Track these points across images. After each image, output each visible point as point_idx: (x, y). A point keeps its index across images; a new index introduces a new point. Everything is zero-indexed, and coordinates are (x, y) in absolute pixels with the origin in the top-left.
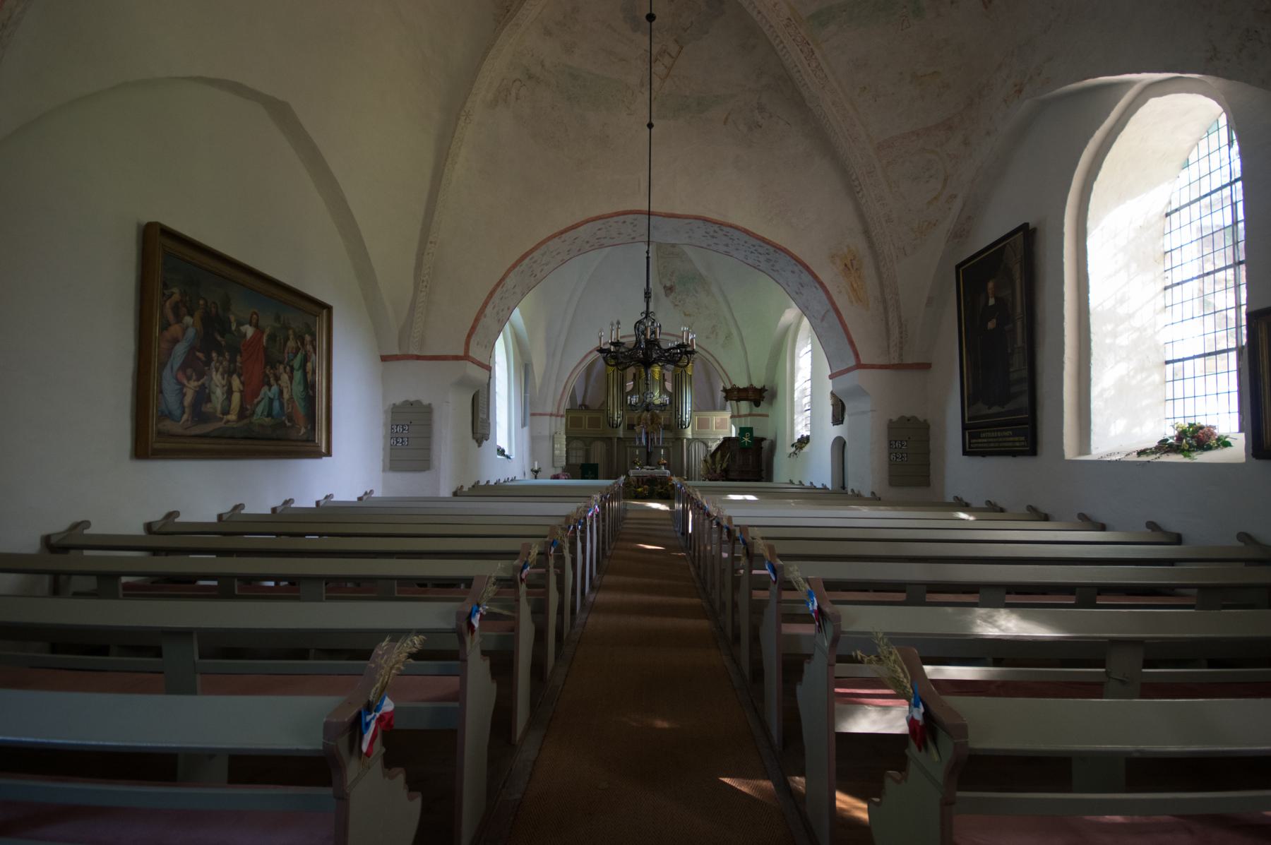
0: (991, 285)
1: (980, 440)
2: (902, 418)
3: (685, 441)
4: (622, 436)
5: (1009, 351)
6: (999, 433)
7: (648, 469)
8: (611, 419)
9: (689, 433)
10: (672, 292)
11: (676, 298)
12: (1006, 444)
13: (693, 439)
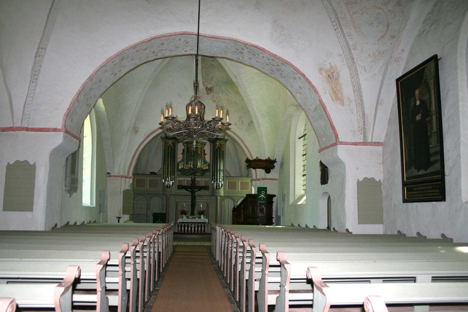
0: (417, 92)
1: (413, 193)
2: (365, 178)
5: (429, 134)
6: (424, 187)
9: (222, 192)
10: (211, 91)
11: (214, 96)
12: (428, 195)
13: (224, 196)
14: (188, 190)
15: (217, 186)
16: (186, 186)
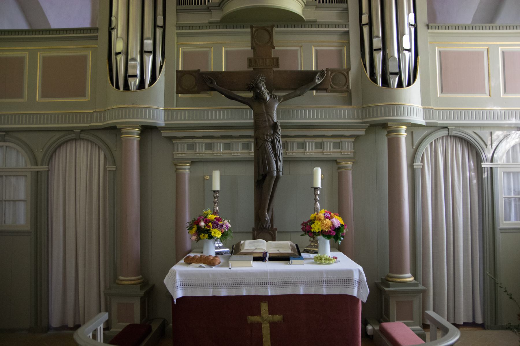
7: (260, 258)
8: (121, 59)
13: (428, 126)
16: (224, 71)
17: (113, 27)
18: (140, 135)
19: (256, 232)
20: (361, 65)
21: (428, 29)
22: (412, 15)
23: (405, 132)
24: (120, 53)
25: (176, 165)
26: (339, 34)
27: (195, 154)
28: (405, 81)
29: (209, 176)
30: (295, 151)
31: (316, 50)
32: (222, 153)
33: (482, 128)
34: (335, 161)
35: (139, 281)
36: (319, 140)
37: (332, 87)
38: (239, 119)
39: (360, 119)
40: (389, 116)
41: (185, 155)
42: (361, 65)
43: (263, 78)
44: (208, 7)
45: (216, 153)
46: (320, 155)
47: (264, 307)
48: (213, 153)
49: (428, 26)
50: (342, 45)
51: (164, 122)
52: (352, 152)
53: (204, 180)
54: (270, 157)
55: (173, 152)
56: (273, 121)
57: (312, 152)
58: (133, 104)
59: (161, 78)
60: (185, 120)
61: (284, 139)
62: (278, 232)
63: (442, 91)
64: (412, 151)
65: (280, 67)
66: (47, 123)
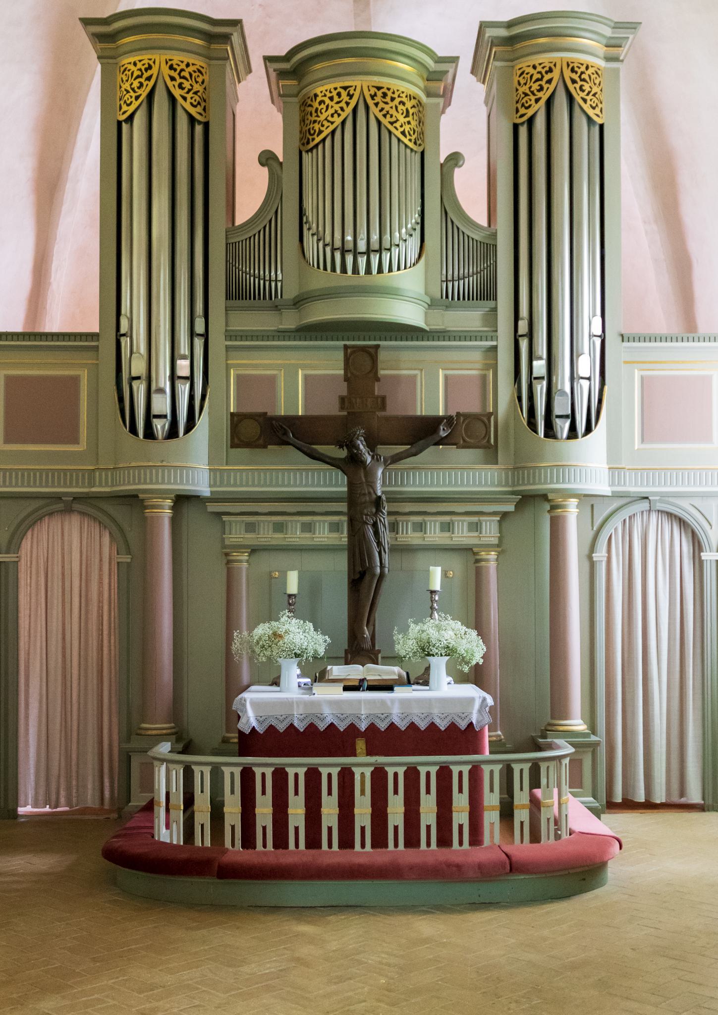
3: (572, 511)
4: (202, 486)
8: (140, 389)
14: (321, 449)
15: (557, 410)
17: (123, 331)
18: (173, 508)
19: (349, 656)
20: (515, 404)
21: (623, 341)
22: (598, 320)
23: (577, 508)
24: (138, 378)
25: (227, 554)
26: (483, 350)
27: (258, 538)
28: (581, 426)
29: (278, 572)
30: (410, 536)
31: (445, 375)
32: (299, 538)
33: (705, 498)
34: (468, 551)
35: (173, 730)
36: (447, 518)
37: (464, 441)
38: (325, 485)
39: (510, 486)
40: (552, 482)
41: (242, 540)
42: (515, 400)
43: (361, 432)
44: (277, 306)
45: (290, 538)
46: (448, 542)
47: (361, 745)
48: (285, 538)
49: (622, 336)
50: (487, 367)
51: (208, 489)
52: (497, 537)
53: (271, 577)
54: (371, 545)
55: (224, 536)
56: (375, 493)
57: (435, 537)
58: (162, 461)
59: (203, 422)
60: (241, 485)
61: (393, 518)
62: (383, 658)
63: (643, 441)
64: (591, 534)
65: (388, 408)
66: (17, 485)
